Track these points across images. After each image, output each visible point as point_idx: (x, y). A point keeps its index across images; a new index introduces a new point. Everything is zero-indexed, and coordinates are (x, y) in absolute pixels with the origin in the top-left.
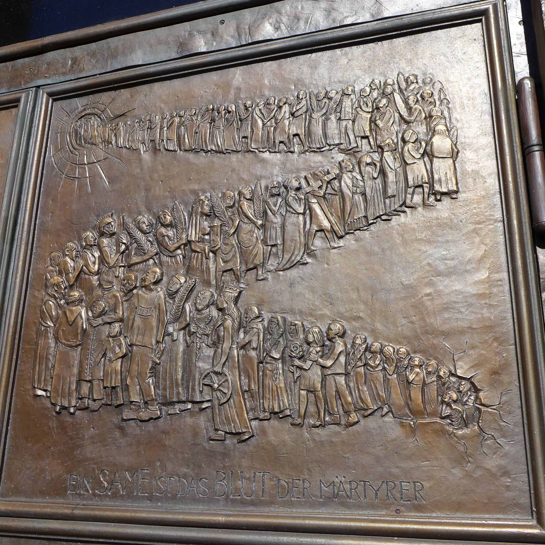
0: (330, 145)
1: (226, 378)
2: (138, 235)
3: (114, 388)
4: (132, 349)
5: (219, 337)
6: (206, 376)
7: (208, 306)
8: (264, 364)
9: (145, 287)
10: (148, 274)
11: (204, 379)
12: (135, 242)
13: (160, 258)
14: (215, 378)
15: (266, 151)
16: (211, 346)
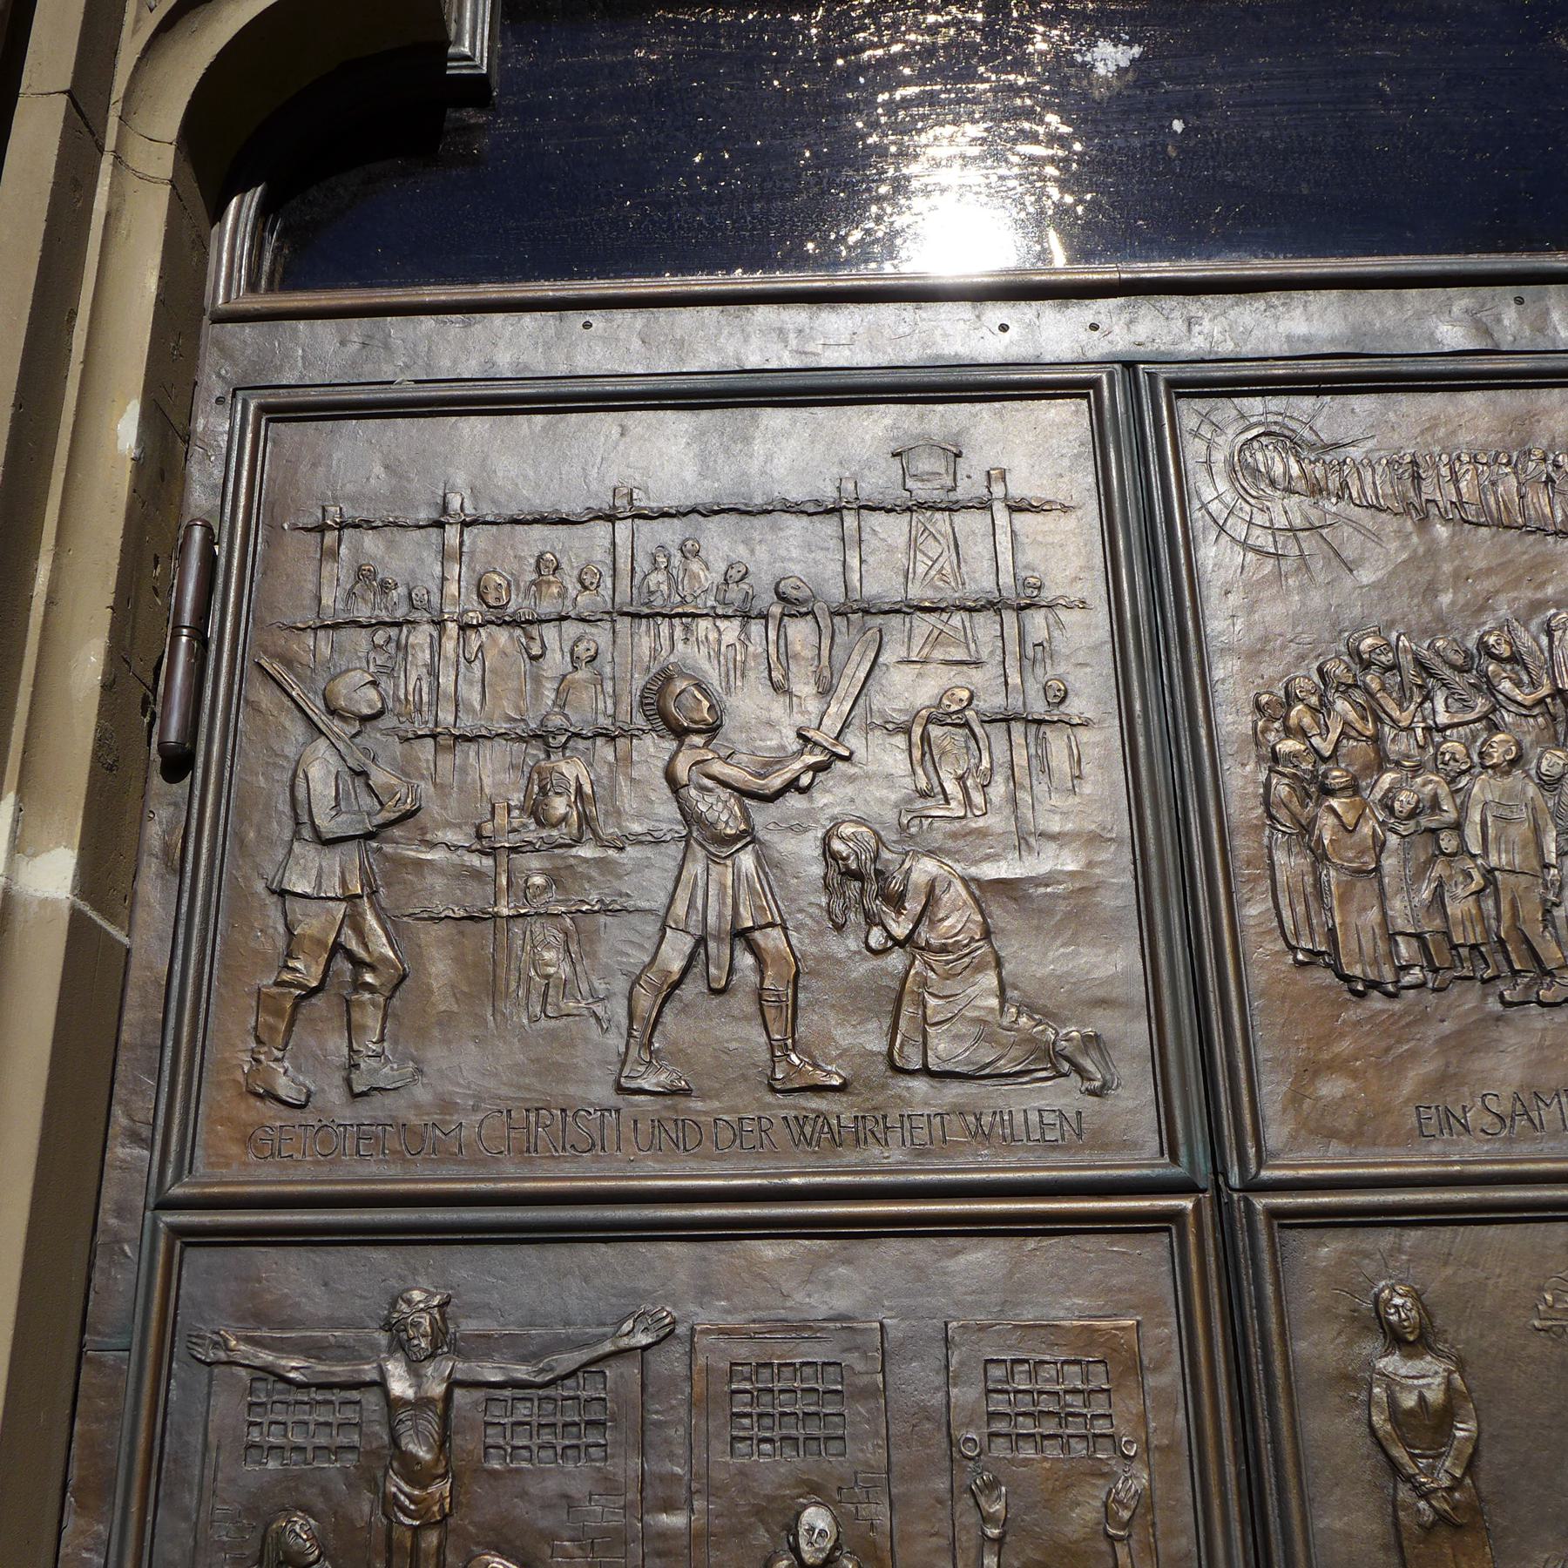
2: (1447, 673)
3: (1474, 947)
9: (1493, 767)
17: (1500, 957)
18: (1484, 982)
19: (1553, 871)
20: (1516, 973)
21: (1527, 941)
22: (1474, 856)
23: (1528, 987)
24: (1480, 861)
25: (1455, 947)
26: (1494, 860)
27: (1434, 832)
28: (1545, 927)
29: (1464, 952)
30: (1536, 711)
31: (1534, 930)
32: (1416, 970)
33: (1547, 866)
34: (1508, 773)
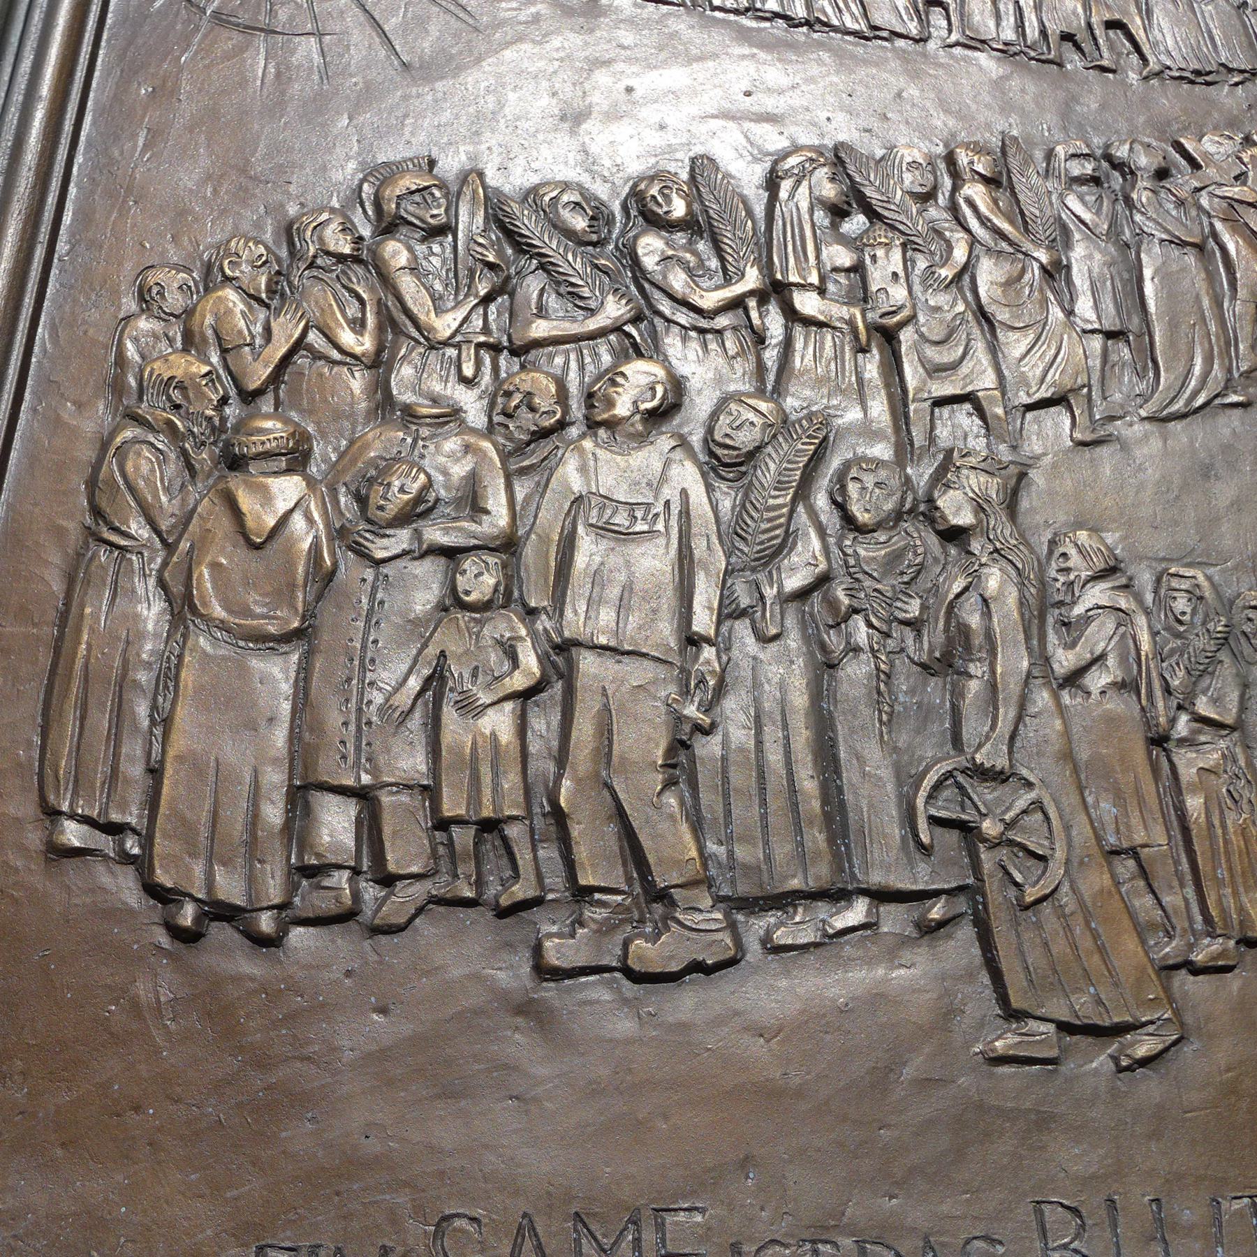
0: (1230, 70)
1: (1032, 795)
2: (551, 245)
3: (490, 826)
4: (571, 665)
5: (964, 630)
6: (937, 787)
7: (899, 515)
8: (1171, 745)
10: (619, 380)
11: (930, 797)
12: (541, 266)
13: (654, 335)
14: (984, 794)
15: (1015, 54)
16: (936, 666)
17: (549, 853)
18: (503, 913)
19: (708, 652)
20: (582, 894)
21: (620, 814)
22: (532, 613)
23: (606, 929)
24: (543, 623)
25: (443, 824)
26: (575, 621)
27: (451, 554)
28: (670, 783)
29: (463, 837)
30: (722, 321)
31: (641, 789)
32: (341, 879)
33: (692, 641)
34: (642, 439)
